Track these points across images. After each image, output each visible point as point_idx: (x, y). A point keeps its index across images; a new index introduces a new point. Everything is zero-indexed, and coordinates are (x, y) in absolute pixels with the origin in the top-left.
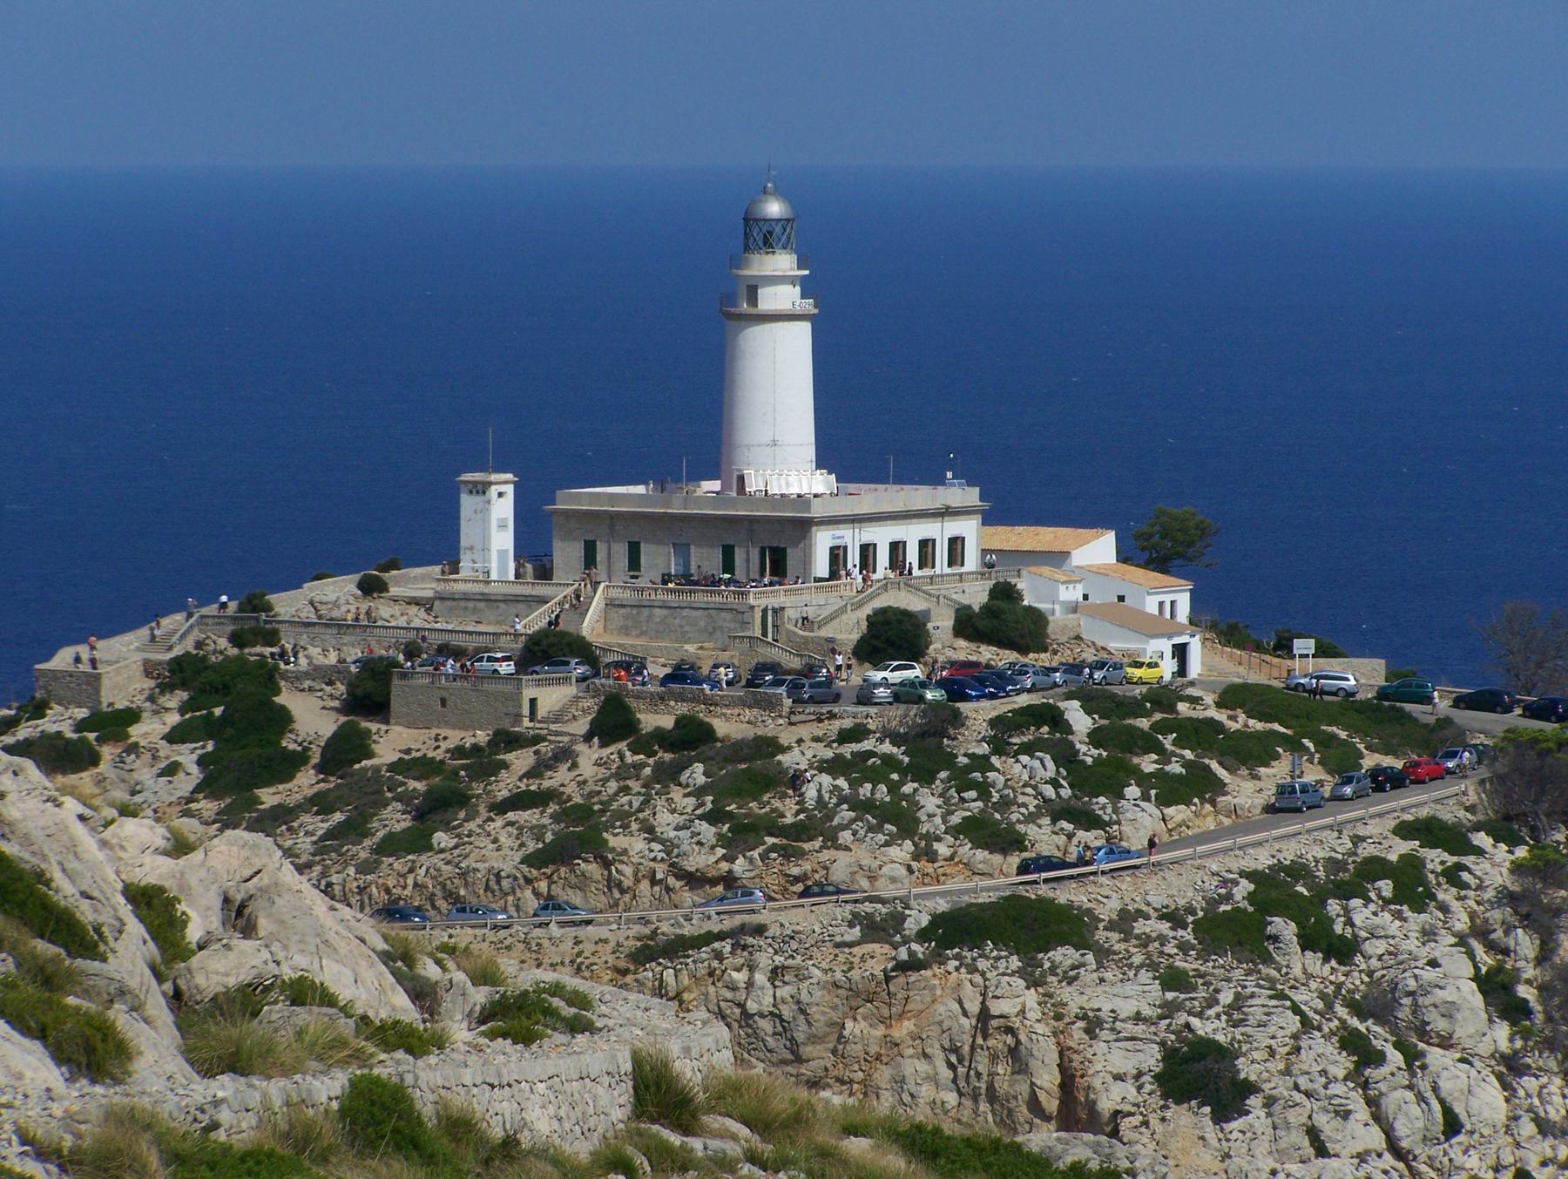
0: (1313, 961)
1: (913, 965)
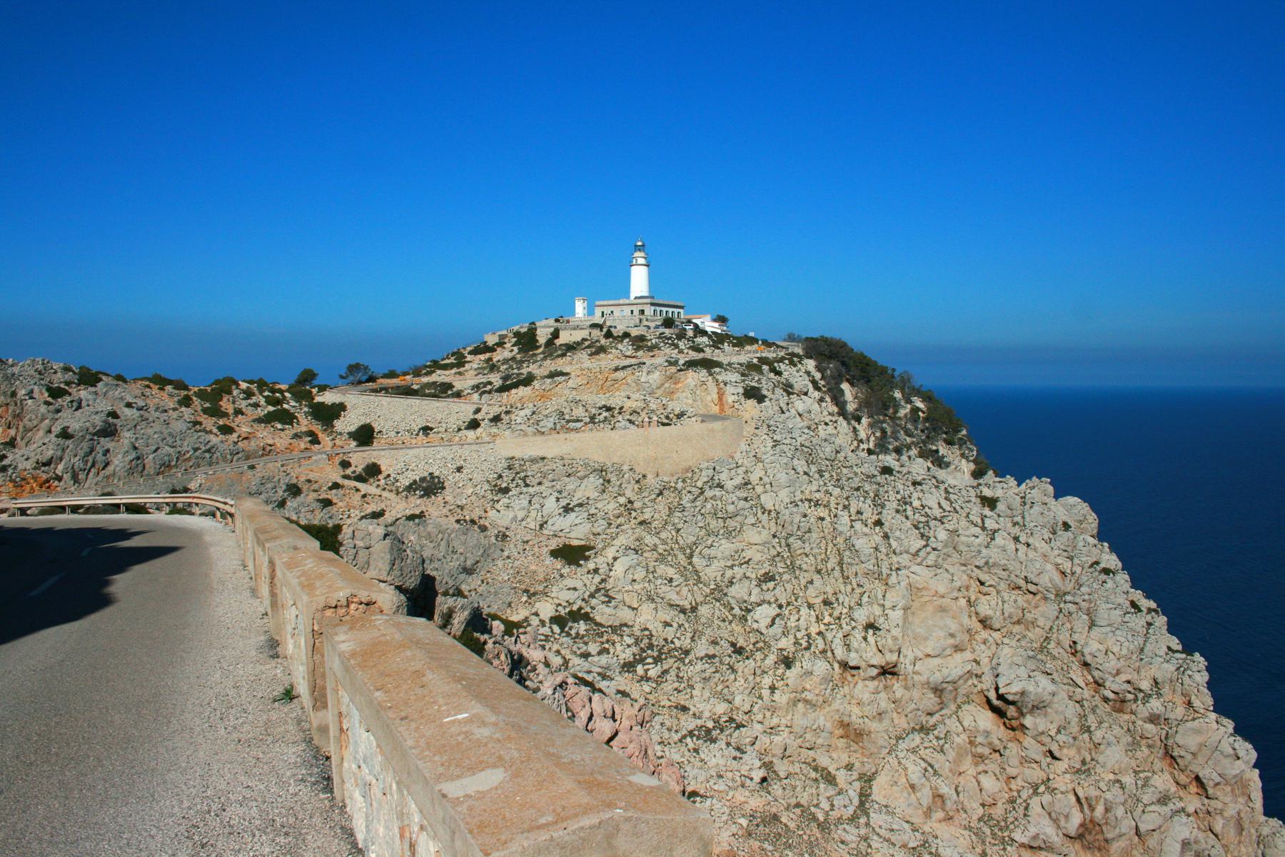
0: (772, 375)
1: (680, 370)
